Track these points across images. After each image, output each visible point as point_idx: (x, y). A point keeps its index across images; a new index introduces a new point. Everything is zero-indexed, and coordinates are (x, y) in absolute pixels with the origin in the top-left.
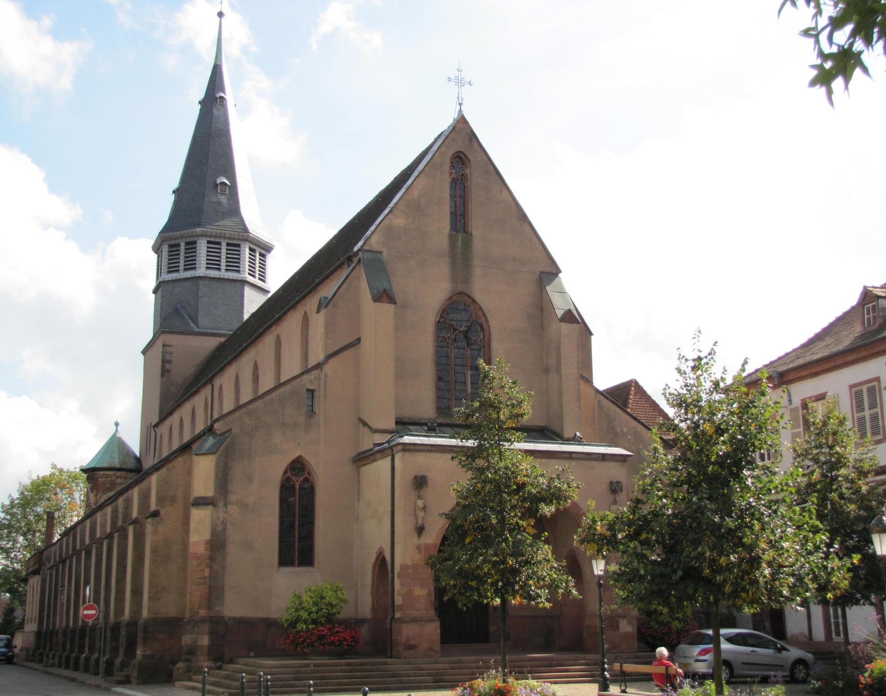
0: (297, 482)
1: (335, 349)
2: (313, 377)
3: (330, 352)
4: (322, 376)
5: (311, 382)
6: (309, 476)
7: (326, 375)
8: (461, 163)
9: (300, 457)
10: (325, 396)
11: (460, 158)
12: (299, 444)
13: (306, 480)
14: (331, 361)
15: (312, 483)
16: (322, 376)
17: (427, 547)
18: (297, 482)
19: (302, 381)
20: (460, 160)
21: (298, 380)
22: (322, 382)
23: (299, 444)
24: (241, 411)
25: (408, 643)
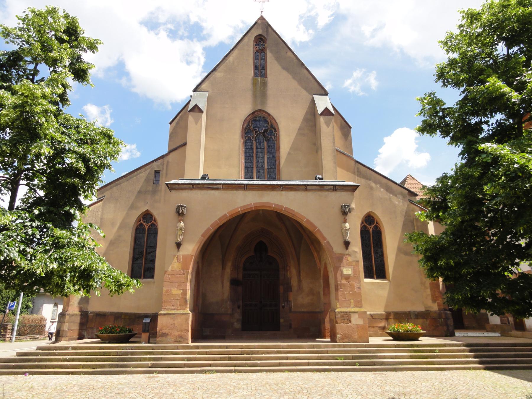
0: (146, 226)
1: (175, 146)
2: (159, 163)
3: (172, 148)
4: (165, 163)
5: (158, 166)
6: (154, 222)
7: (168, 162)
8: (262, 42)
9: (147, 210)
10: (166, 174)
11: (261, 39)
12: (147, 203)
13: (153, 225)
14: (171, 154)
15: (156, 227)
16: (165, 163)
17: (185, 257)
18: (146, 226)
19: (152, 166)
20: (260, 40)
21: (150, 166)
22: (165, 167)
23: (147, 203)
24: (111, 185)
25: (161, 332)
